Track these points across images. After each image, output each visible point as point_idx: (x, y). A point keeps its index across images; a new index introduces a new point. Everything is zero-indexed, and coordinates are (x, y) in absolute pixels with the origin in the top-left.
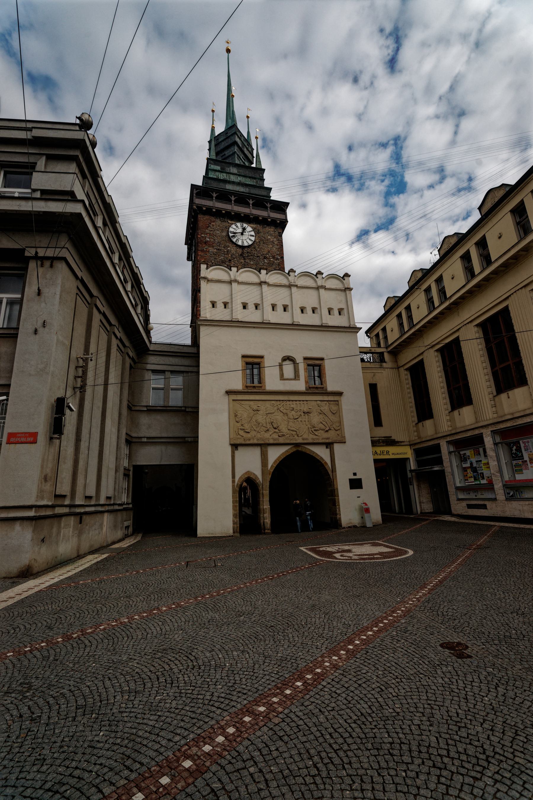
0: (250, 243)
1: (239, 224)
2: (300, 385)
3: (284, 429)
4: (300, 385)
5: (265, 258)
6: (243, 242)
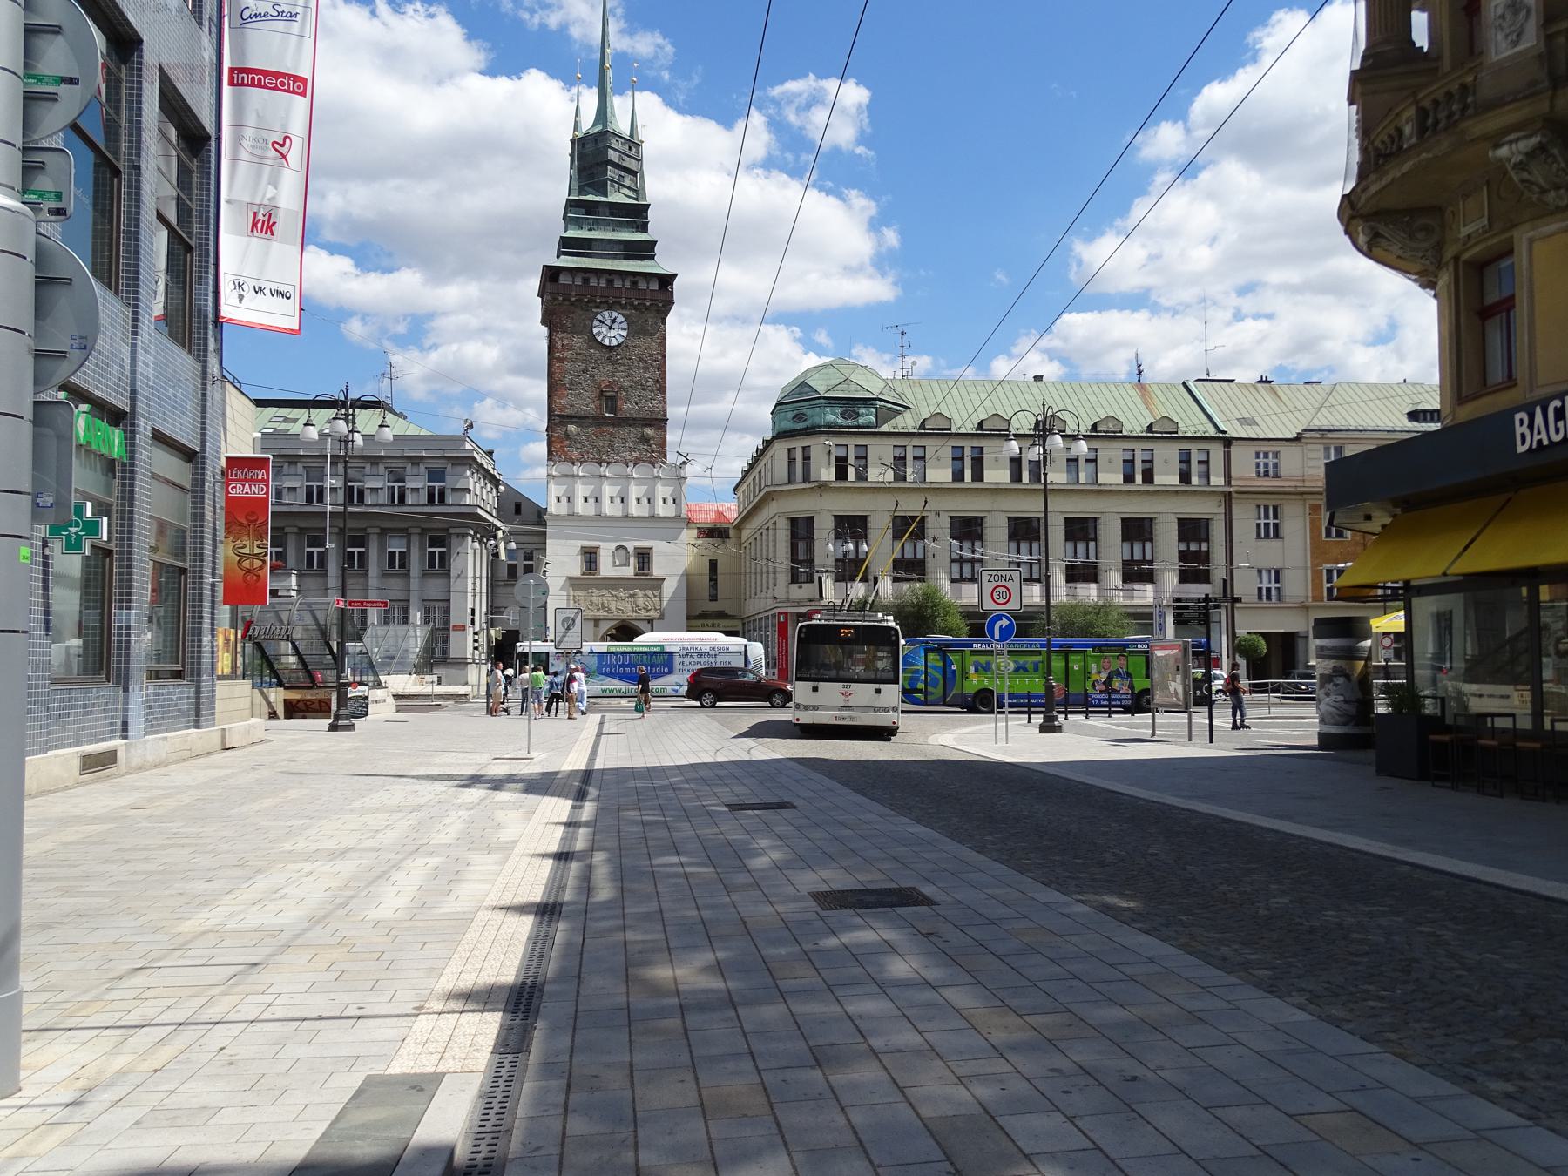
0: (621, 340)
1: (606, 314)
2: (629, 571)
3: (614, 609)
4: (629, 571)
5: (640, 359)
6: (611, 341)
